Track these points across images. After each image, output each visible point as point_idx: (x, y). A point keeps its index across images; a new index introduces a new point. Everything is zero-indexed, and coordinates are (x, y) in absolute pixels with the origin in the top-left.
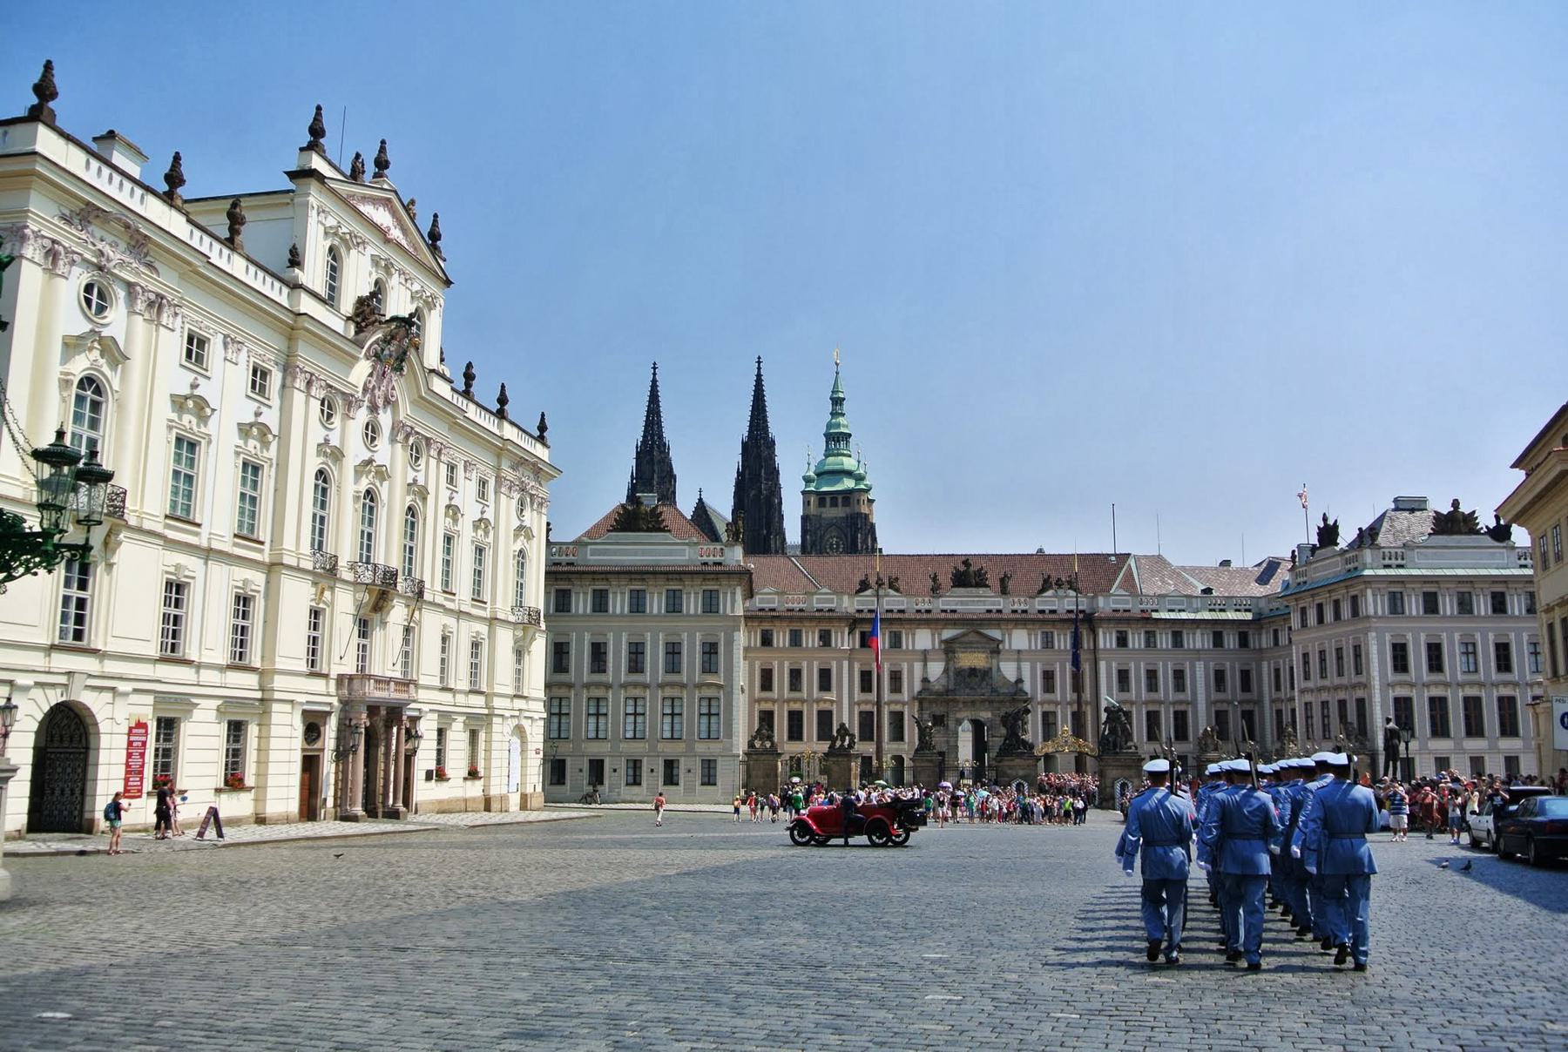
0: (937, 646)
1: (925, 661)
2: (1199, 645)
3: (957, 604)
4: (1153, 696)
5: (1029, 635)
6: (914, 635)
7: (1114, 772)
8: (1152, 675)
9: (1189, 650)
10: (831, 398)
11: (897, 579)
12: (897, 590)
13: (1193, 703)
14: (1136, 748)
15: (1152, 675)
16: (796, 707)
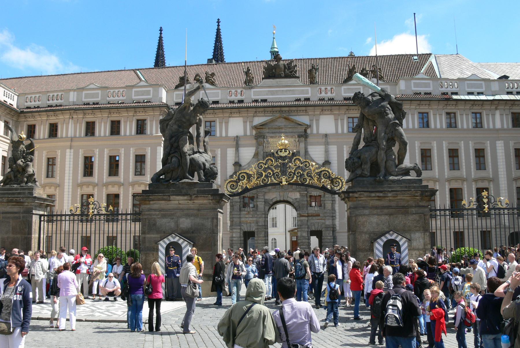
0: (248, 133)
1: (237, 147)
2: (498, 125)
3: (267, 95)
4: (456, 173)
5: (336, 120)
6: (227, 123)
7: (374, 219)
8: (453, 154)
9: (489, 129)
10: (271, 52)
11: (213, 75)
12: (212, 84)
13: (495, 180)
14: (419, 174)
15: (453, 154)
16: (113, 190)
